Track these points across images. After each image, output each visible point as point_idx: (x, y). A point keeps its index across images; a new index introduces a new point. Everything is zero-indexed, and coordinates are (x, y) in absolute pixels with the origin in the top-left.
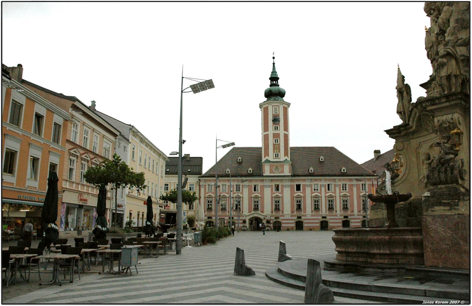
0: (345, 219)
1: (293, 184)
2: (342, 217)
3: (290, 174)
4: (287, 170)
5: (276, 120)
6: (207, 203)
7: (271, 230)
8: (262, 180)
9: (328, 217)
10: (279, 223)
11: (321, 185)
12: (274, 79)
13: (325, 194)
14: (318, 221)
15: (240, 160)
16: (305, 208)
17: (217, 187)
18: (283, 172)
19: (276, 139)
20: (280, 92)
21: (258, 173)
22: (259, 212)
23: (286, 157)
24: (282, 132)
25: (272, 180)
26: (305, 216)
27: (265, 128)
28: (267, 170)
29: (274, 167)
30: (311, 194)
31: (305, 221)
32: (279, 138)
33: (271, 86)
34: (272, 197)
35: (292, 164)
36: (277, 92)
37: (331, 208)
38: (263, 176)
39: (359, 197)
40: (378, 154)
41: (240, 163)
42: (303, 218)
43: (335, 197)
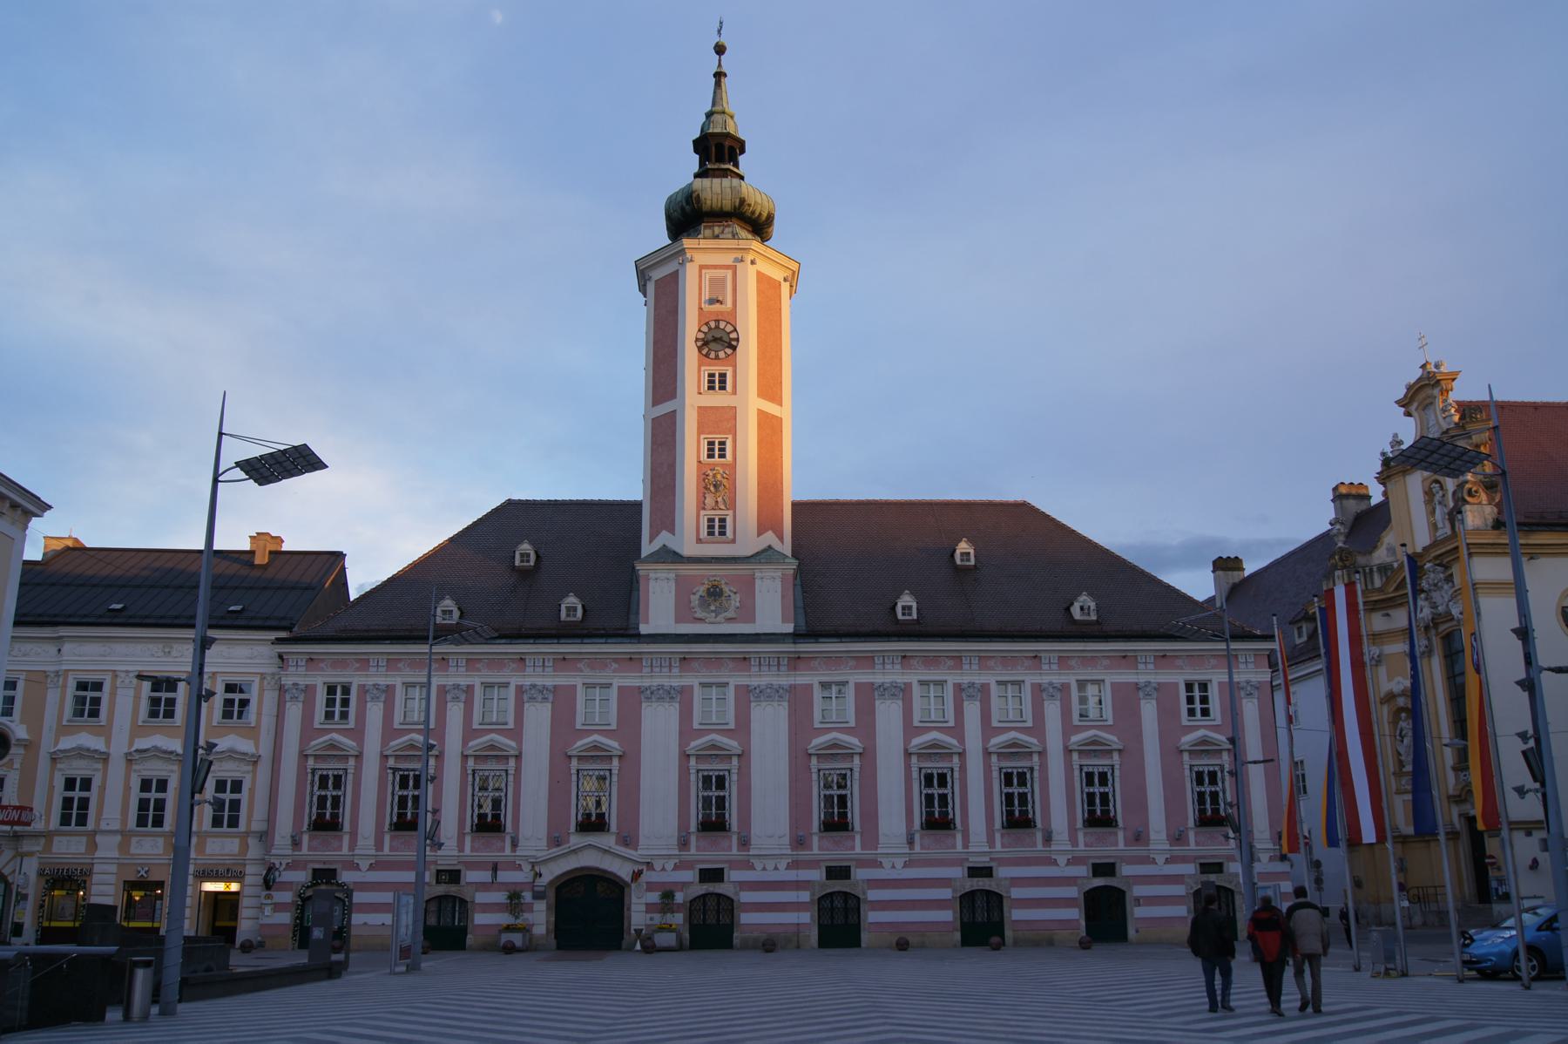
0: (1099, 882)
1: (801, 679)
2: (1082, 871)
3: (789, 628)
4: (771, 608)
5: (719, 341)
6: (393, 791)
7: (680, 948)
9: (1002, 872)
10: (726, 905)
11: (959, 688)
12: (718, 150)
15: (525, 556)
16: (871, 816)
17: (338, 696)
18: (748, 613)
19: (717, 438)
20: (742, 201)
21: (613, 619)
22: (607, 840)
23: (770, 538)
24: (750, 403)
26: (875, 864)
27: (664, 381)
28: (660, 606)
29: (702, 590)
30: (907, 740)
31: (873, 895)
33: (697, 176)
35: (801, 572)
36: (728, 207)
37: (1018, 818)
39: (1171, 752)
40: (1236, 577)
41: (525, 574)
42: (859, 874)
43: (1042, 754)
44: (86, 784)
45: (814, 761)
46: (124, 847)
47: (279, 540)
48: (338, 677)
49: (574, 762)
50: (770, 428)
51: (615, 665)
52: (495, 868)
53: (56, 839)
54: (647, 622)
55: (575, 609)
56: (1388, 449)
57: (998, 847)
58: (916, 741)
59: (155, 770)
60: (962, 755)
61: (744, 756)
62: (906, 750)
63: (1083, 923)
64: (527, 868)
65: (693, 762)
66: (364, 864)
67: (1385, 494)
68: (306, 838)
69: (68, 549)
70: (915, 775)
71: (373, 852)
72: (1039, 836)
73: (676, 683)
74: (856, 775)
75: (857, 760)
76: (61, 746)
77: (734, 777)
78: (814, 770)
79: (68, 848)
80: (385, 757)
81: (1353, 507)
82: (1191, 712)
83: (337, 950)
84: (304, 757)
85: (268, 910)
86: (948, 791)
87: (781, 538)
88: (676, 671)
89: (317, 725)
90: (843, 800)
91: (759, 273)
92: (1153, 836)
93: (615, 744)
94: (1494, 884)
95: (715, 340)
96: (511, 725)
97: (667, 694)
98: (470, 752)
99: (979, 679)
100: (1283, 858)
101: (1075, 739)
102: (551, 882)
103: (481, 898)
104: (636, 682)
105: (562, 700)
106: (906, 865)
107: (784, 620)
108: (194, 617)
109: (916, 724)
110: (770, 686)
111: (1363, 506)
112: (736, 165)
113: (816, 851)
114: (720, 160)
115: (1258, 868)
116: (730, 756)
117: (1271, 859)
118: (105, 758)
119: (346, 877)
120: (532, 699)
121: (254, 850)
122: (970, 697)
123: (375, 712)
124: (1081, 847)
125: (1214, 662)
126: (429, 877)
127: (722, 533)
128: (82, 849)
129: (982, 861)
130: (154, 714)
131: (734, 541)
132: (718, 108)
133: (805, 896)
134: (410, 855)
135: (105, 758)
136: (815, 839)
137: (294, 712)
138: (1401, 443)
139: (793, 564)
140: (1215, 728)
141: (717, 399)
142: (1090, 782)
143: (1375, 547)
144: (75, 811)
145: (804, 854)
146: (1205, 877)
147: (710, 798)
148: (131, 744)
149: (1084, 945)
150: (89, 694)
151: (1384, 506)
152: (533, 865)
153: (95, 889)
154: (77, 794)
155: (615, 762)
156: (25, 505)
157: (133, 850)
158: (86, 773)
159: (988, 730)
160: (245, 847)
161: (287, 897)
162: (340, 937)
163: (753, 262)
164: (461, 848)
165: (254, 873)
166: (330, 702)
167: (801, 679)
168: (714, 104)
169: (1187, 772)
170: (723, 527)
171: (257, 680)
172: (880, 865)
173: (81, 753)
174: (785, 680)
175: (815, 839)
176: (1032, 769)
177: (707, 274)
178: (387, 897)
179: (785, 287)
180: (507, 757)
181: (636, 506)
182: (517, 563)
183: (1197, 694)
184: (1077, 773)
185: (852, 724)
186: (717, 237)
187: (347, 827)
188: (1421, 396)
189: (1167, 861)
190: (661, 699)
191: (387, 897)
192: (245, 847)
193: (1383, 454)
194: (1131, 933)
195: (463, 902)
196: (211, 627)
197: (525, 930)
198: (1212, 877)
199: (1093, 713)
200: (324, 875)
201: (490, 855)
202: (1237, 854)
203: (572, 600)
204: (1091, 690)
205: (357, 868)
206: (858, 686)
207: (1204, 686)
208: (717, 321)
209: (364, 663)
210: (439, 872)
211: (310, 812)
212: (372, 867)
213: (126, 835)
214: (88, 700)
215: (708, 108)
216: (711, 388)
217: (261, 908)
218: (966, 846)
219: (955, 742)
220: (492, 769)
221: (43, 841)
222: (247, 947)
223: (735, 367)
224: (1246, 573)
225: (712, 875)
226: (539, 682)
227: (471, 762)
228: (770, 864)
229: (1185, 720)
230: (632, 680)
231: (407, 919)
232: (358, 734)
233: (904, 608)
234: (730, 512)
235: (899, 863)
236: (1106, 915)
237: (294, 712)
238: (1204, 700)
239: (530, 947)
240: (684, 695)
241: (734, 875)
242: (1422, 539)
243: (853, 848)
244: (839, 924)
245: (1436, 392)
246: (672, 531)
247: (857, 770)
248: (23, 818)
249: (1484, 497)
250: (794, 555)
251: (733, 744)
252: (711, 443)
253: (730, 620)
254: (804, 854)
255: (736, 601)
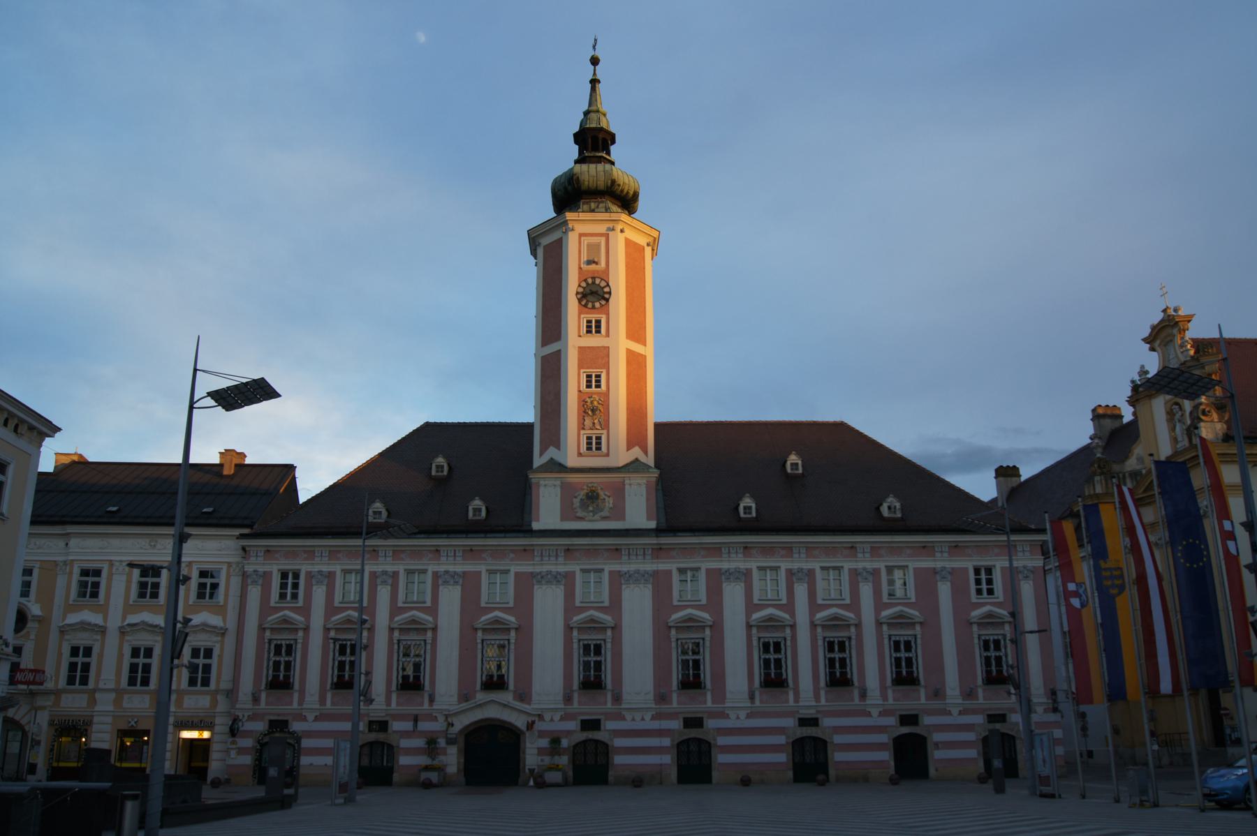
0: (905, 730)
1: (662, 566)
2: (891, 721)
3: (652, 525)
4: (638, 509)
5: (595, 294)
7: (565, 784)
8: (527, 551)
9: (827, 722)
10: (603, 749)
11: (790, 573)
12: (594, 141)
13: (812, 614)
14: (781, 740)
15: (440, 468)
16: (719, 677)
18: (619, 512)
19: (594, 372)
20: (613, 182)
21: (511, 517)
22: (506, 697)
23: (636, 452)
25: (568, 550)
26: (723, 715)
27: (551, 325)
29: (582, 494)
30: (748, 615)
32: (607, 366)
33: (576, 162)
34: (569, 629)
35: (661, 479)
36: (601, 185)
37: (839, 678)
38: (530, 532)
39: (963, 624)
40: (1013, 482)
41: (440, 482)
42: (710, 724)
44: (88, 651)
45: (673, 632)
46: (118, 702)
47: (243, 455)
48: (289, 566)
49: (480, 634)
50: (636, 364)
51: (512, 555)
52: (416, 720)
53: (63, 696)
54: (538, 520)
55: (480, 510)
56: (1137, 378)
57: (823, 701)
58: (756, 616)
59: (143, 640)
60: (793, 627)
61: (616, 628)
62: (748, 623)
63: (892, 763)
64: (441, 719)
65: (575, 633)
66: (311, 717)
67: (1134, 414)
68: (263, 695)
69: (74, 462)
70: (755, 643)
71: (317, 706)
72: (856, 693)
73: (562, 569)
74: (708, 644)
75: (708, 632)
76: (68, 621)
77: (609, 645)
78: (673, 639)
79: (73, 703)
80: (327, 630)
81: (1109, 424)
82: (979, 592)
83: (288, 786)
84: (262, 629)
85: (233, 753)
86: (781, 656)
87: (646, 453)
88: (561, 559)
89: (272, 604)
90: (696, 663)
91: (627, 240)
92: (949, 692)
93: (512, 619)
94: (1228, 731)
95: (592, 293)
96: (429, 604)
97: (555, 578)
98: (395, 626)
99: (806, 566)
100: (1055, 710)
101: (885, 613)
102: (461, 731)
103: (405, 743)
104: (530, 569)
105: (470, 584)
106: (748, 716)
107: (649, 519)
108: (173, 517)
109: (756, 602)
110: (637, 572)
111: (1116, 424)
112: (608, 153)
113: (675, 705)
114: (595, 149)
115: (1035, 718)
116: (703, 627)
117: (1046, 711)
118: (102, 630)
119: (296, 726)
120: (446, 582)
121: (222, 705)
122: (800, 580)
123: (319, 593)
124: (891, 701)
125: (996, 550)
126: (362, 726)
127: (599, 449)
128: (84, 704)
129: (810, 713)
130: (142, 595)
131: (607, 455)
132: (593, 108)
133: (666, 742)
134: (348, 709)
135: (102, 630)
136: (675, 696)
137: (254, 593)
138: (1147, 372)
139: (655, 474)
140: (999, 605)
141: (593, 341)
142: (897, 649)
143: (1127, 457)
144: (79, 673)
145: (665, 708)
146: (991, 726)
147: (589, 662)
148: (124, 618)
149: (893, 781)
150: (91, 579)
151: (1134, 423)
152: (447, 716)
153: (94, 736)
154: (80, 660)
155: (513, 633)
156: (43, 428)
157: (125, 705)
158: (88, 643)
159: (814, 607)
160: (214, 703)
161: (248, 743)
162: (291, 775)
163: (622, 231)
164: (388, 703)
165: (222, 723)
166: (283, 586)
167: (662, 566)
168: (590, 105)
169: (976, 641)
170: (599, 443)
171: (225, 567)
172: (727, 717)
173: (84, 626)
174: (650, 566)
175: (675, 696)
176: (850, 638)
177: (585, 240)
178: (328, 743)
179: (648, 251)
180: (425, 630)
181: (529, 426)
182: (433, 473)
183: (983, 577)
184: (886, 641)
185: (704, 602)
186: (593, 211)
187: (296, 686)
188: (1163, 335)
189: (960, 713)
190: (549, 582)
191: (328, 743)
192: (214, 703)
193: (1133, 382)
194: (932, 771)
195: (390, 747)
196: (187, 525)
197: (440, 769)
198: (998, 726)
199: (899, 593)
200: (278, 725)
201: (413, 709)
202: (1017, 707)
203: (477, 503)
204: (898, 574)
205: (304, 719)
206: (708, 570)
207: (989, 571)
208: (594, 278)
209: (310, 554)
210: (371, 723)
211: (267, 674)
212: (316, 719)
213: (119, 692)
214: (90, 584)
215: (586, 108)
216: (589, 332)
217: (227, 751)
218: (797, 700)
219: (787, 616)
220: (414, 639)
221: (52, 697)
222: (216, 783)
223: (608, 315)
224: (1023, 479)
225: (591, 725)
226: (451, 568)
227: (396, 634)
228: (638, 716)
229: (974, 598)
230: (526, 567)
231: (345, 760)
232: (306, 611)
233: (745, 508)
234: (605, 432)
235: (743, 714)
236: (911, 758)
237: (254, 593)
238: (990, 582)
239: (445, 783)
240: (567, 580)
241: (609, 725)
242: (1165, 451)
243: (705, 703)
244: (694, 763)
245: (1175, 331)
246: (558, 447)
247: (707, 639)
248: (37, 679)
249: (1215, 416)
250: (656, 466)
251: (607, 618)
252: (589, 376)
253: (604, 518)
254: (665, 708)
255: (610, 502)
